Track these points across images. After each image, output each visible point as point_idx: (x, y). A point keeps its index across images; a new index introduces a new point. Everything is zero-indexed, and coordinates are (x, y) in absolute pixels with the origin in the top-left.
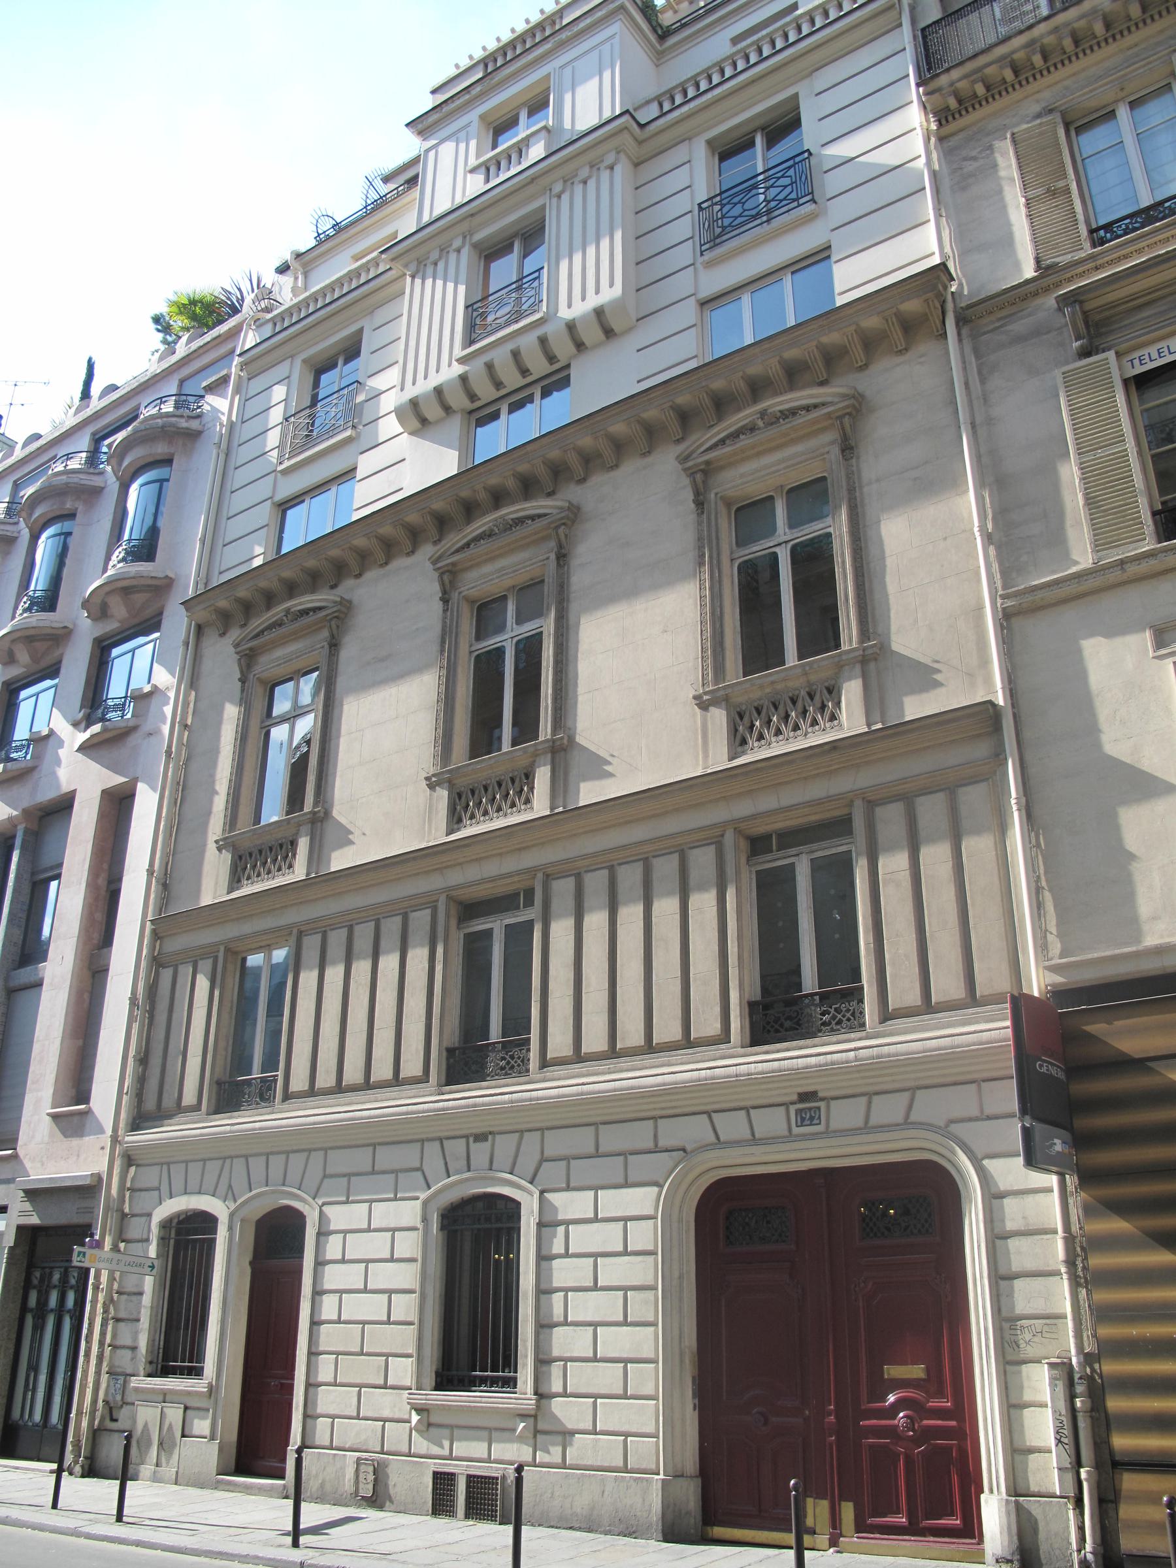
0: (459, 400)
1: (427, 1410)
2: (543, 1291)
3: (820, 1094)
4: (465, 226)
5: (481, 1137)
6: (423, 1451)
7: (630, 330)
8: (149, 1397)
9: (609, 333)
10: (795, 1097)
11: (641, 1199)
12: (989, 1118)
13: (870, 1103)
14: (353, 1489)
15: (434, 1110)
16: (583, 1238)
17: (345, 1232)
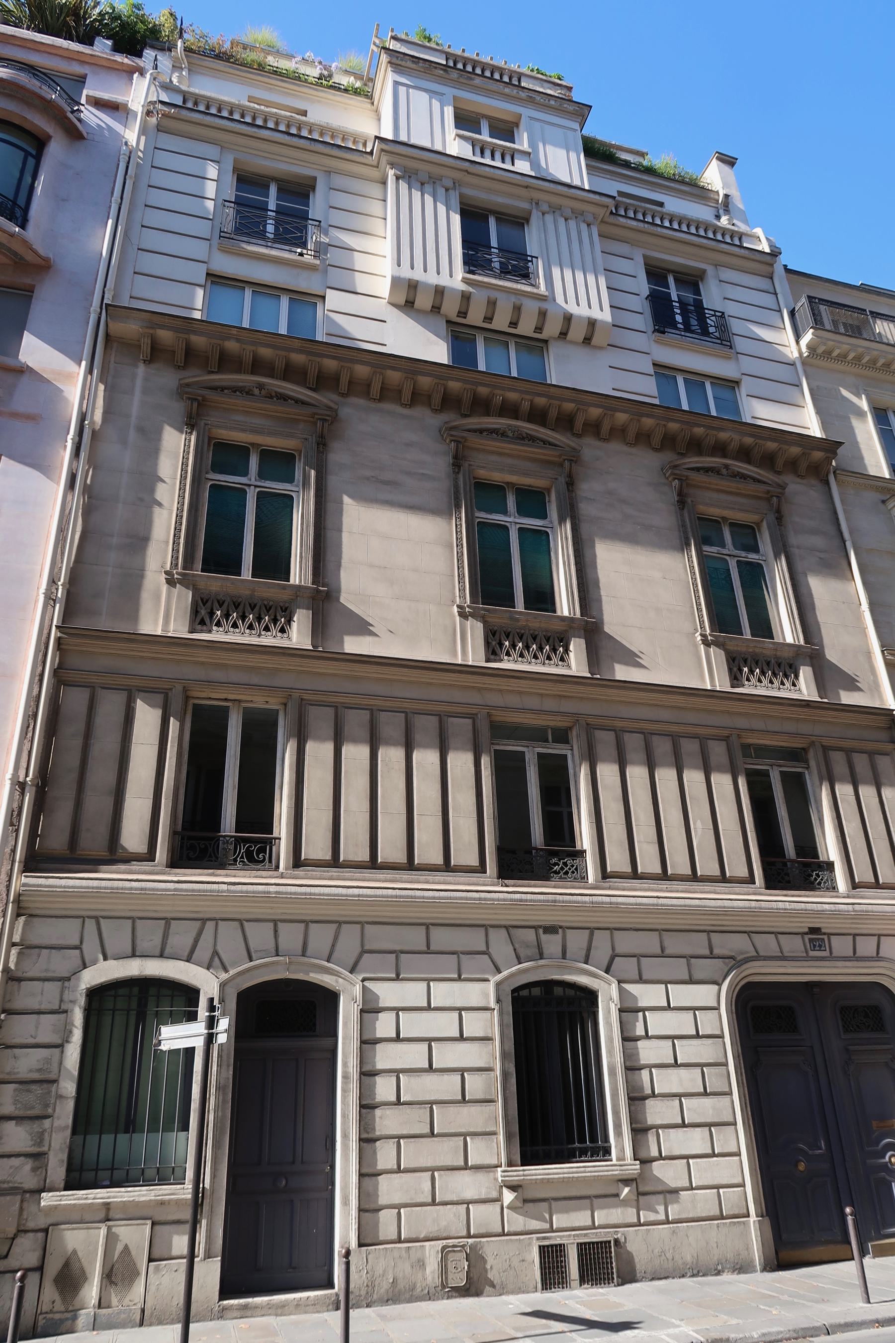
0: (451, 308)
1: (520, 1186)
2: (632, 1067)
3: (823, 931)
4: (458, 175)
5: (551, 930)
6: (519, 1228)
7: (601, 348)
8: (81, 1218)
9: (587, 340)
10: (807, 930)
11: (703, 994)
14: (438, 1282)
15: (511, 900)
16: (658, 1023)
17: (397, 1010)
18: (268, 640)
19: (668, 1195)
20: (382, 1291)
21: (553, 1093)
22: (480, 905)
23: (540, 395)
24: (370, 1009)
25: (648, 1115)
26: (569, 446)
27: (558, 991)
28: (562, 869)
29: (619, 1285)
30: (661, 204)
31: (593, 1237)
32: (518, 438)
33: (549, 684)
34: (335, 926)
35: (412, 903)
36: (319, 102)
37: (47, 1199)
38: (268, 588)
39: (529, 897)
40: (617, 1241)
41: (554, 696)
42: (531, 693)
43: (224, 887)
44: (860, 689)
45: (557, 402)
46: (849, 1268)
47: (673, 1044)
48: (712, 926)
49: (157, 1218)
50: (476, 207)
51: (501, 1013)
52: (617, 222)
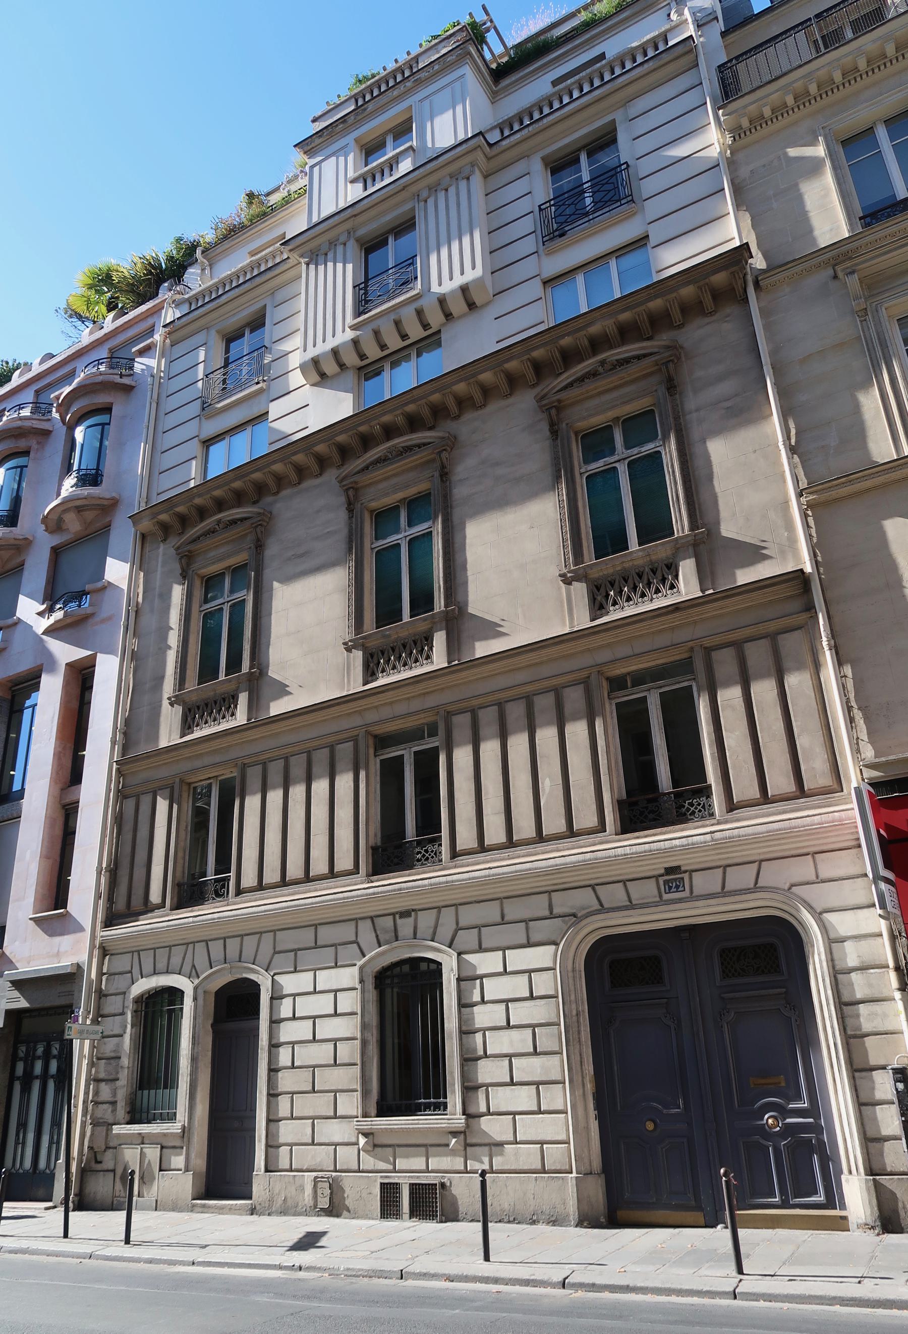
0: (351, 359)
1: (372, 1134)
2: (466, 1031)
3: (683, 869)
4: (348, 225)
5: (405, 914)
6: (371, 1168)
7: (488, 303)
8: (130, 1140)
9: (472, 306)
10: (662, 871)
11: (541, 956)
12: (823, 881)
13: (724, 873)
14: (312, 1203)
15: (367, 895)
16: (495, 988)
17: (294, 996)
18: (660, 602)
19: (493, 1148)
20: (278, 1205)
21: (410, 1055)
22: (344, 903)
23: (406, 404)
24: (277, 997)
25: (479, 1074)
26: (435, 438)
27: (423, 966)
28: (424, 856)
29: (441, 1222)
30: (602, 56)
31: (425, 1178)
32: (397, 456)
33: (411, 687)
34: (239, 939)
35: (297, 911)
36: (292, 216)
37: (116, 1130)
38: (660, 549)
39: (380, 889)
40: (443, 1185)
41: (420, 695)
42: (400, 700)
43: (191, 919)
44: (766, 557)
45: (424, 401)
46: (721, 1235)
47: (516, 1008)
48: (552, 887)
49: (164, 1144)
50: (377, 237)
51: (363, 991)
52: (502, 149)
